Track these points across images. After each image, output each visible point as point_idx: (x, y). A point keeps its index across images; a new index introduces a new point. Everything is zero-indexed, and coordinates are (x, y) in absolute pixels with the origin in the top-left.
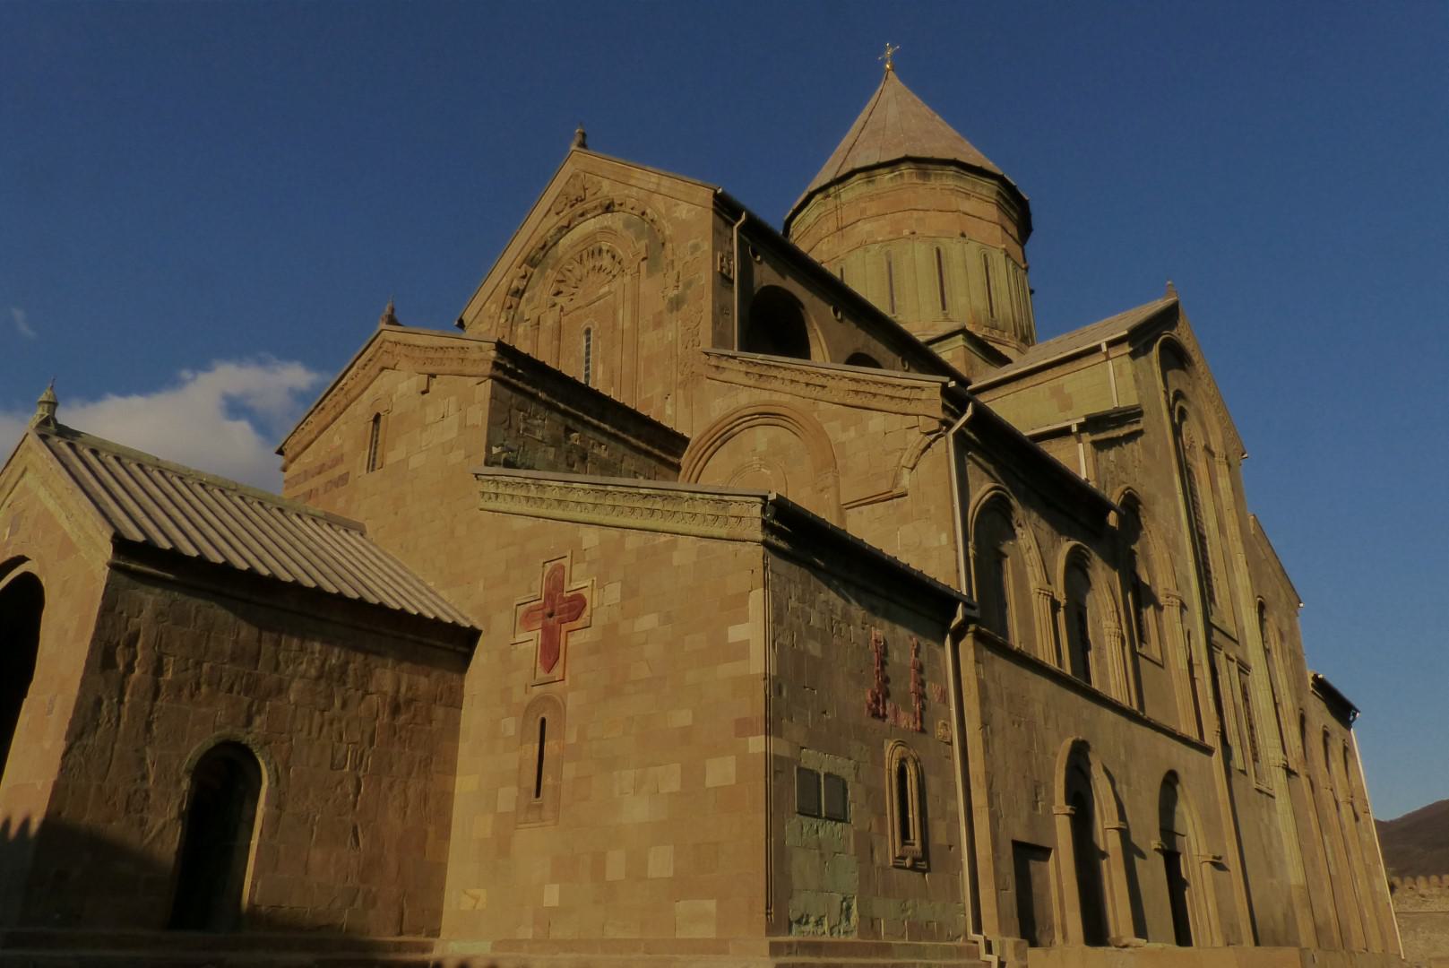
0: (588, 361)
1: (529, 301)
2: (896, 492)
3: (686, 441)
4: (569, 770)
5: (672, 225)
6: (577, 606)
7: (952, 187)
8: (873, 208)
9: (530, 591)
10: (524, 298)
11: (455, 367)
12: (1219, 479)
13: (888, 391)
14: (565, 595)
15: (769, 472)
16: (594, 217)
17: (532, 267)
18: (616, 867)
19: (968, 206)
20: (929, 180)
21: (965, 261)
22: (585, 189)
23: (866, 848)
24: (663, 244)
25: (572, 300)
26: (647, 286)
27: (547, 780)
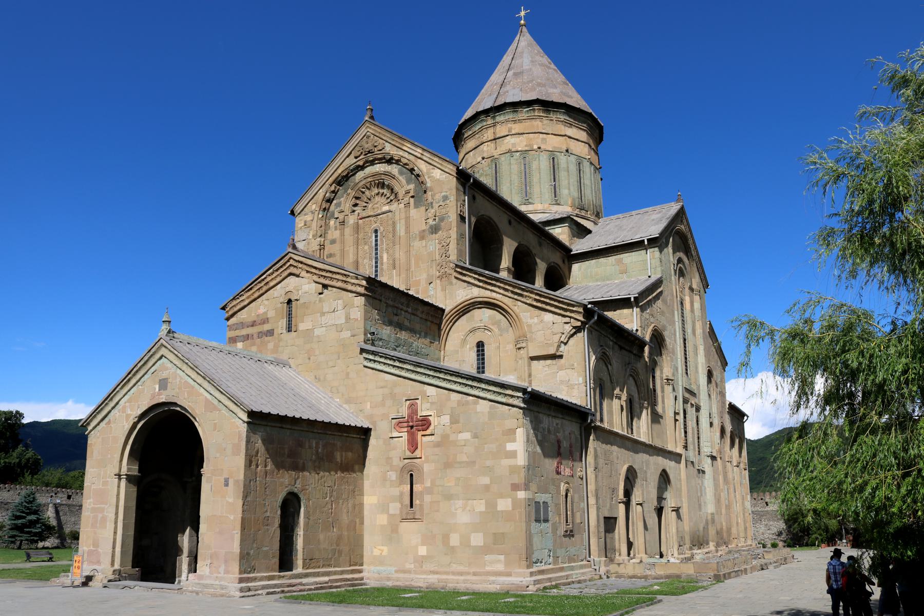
0: (376, 249)
1: (338, 205)
2: (558, 354)
3: (443, 310)
4: (427, 498)
5: (431, 180)
6: (425, 423)
8: (516, 128)
9: (398, 412)
11: (339, 284)
12: (695, 303)
14: (419, 417)
15: (490, 333)
16: (379, 163)
18: (455, 540)
20: (550, 114)
21: (568, 167)
23: (555, 529)
24: (425, 192)
25: (364, 210)
26: (413, 212)
27: (416, 502)
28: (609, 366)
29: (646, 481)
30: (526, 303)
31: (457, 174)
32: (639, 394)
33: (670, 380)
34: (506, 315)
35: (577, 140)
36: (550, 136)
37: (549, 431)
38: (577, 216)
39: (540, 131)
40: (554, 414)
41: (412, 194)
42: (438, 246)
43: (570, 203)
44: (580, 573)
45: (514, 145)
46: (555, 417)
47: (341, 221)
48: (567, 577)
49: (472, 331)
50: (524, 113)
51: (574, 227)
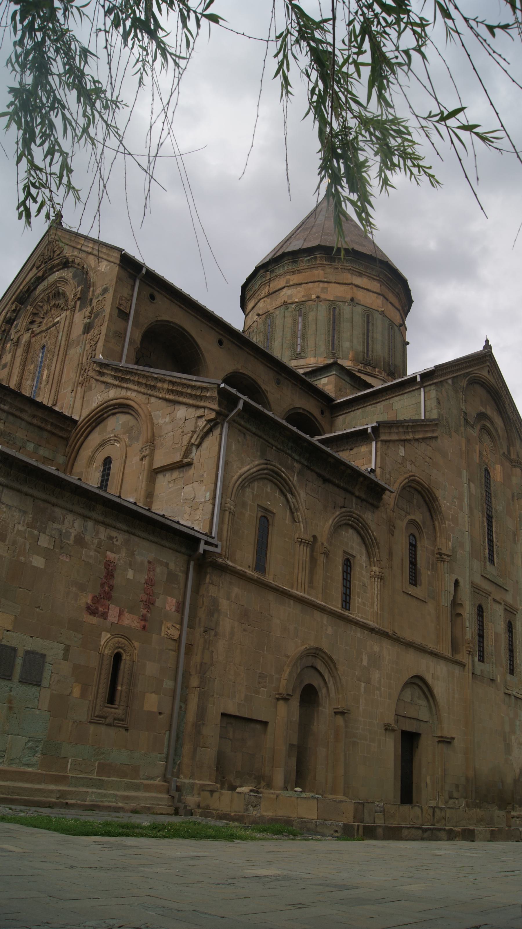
2: (185, 461)
3: (76, 422)
7: (349, 268)
8: (295, 279)
10: (14, 326)
13: (189, 391)
15: (118, 445)
16: (58, 271)
17: (20, 304)
19: (358, 281)
20: (334, 262)
21: (352, 318)
22: (54, 252)
28: (289, 496)
29: (368, 682)
30: (160, 398)
31: (121, 261)
32: (369, 557)
33: (445, 555)
34: (138, 419)
35: (368, 290)
36: (333, 285)
37: (80, 541)
38: (359, 371)
39: (320, 279)
40: (101, 518)
41: (78, 296)
42: (88, 346)
43: (350, 356)
44: (117, 795)
45: (290, 297)
46: (107, 525)
47: (15, 341)
48: (63, 794)
49: (103, 444)
50: (304, 262)
51: (347, 379)
